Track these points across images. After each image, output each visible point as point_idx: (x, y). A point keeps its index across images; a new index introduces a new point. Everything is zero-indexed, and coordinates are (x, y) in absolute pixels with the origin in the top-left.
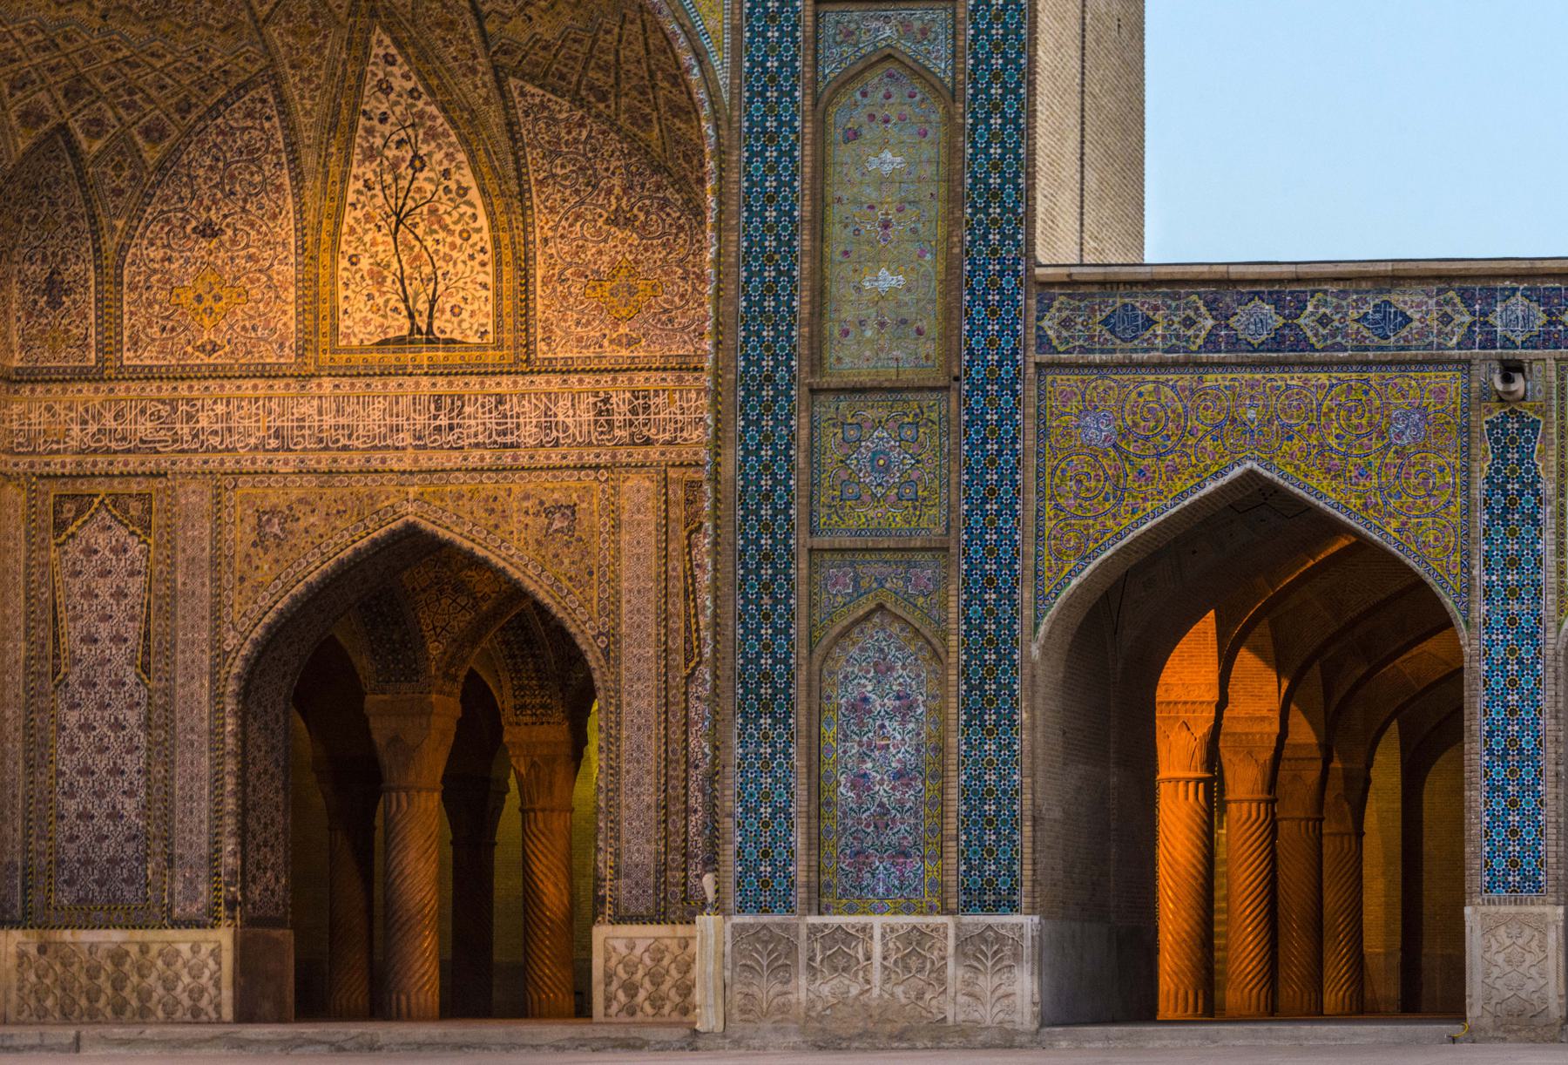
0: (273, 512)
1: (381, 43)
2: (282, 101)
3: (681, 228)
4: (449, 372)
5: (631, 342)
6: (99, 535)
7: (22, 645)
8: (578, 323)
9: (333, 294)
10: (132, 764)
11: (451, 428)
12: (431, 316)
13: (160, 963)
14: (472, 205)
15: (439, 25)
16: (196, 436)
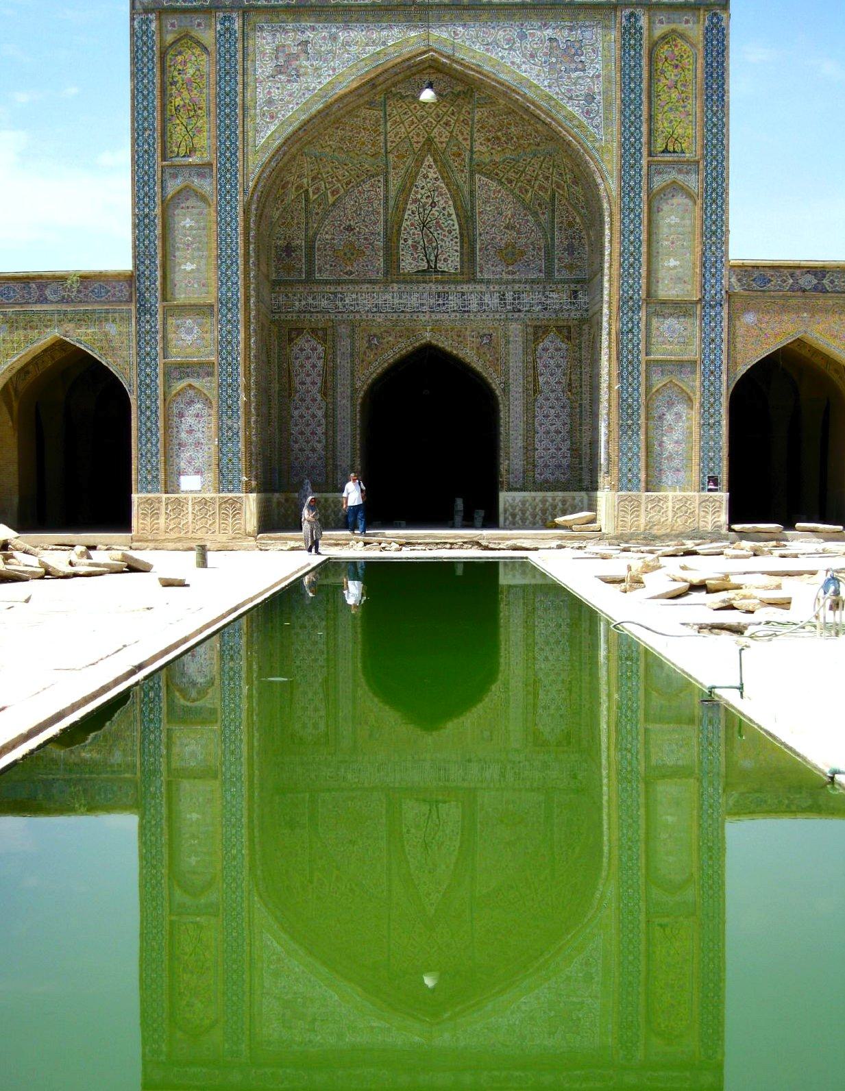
0: (375, 336)
1: (429, 160)
2: (386, 181)
3: (533, 231)
4: (442, 282)
5: (514, 273)
6: (305, 343)
7: (277, 385)
8: (493, 266)
9: (398, 253)
10: (320, 430)
11: (444, 304)
12: (436, 262)
13: (332, 505)
14: (453, 220)
15: (454, 155)
16: (344, 306)
